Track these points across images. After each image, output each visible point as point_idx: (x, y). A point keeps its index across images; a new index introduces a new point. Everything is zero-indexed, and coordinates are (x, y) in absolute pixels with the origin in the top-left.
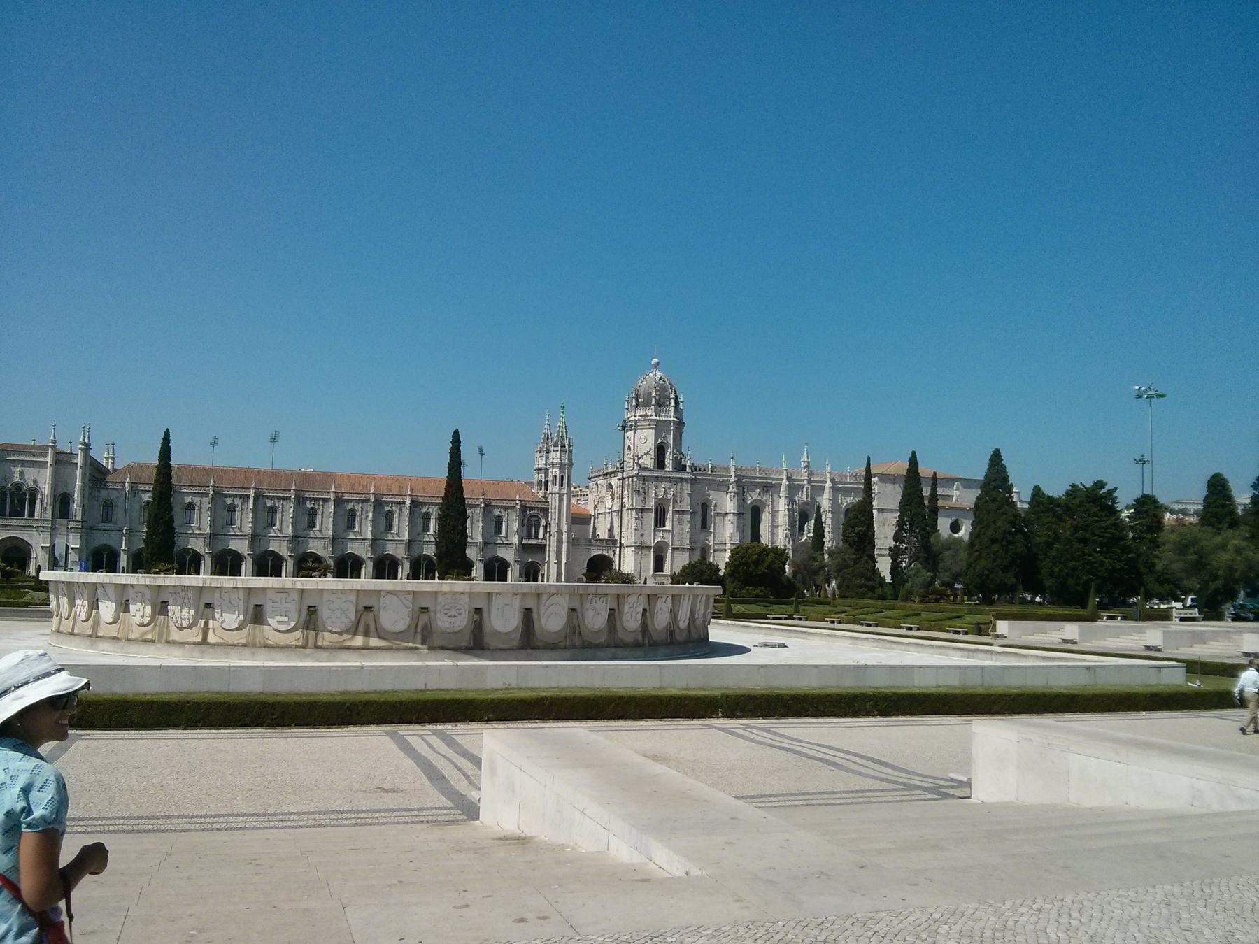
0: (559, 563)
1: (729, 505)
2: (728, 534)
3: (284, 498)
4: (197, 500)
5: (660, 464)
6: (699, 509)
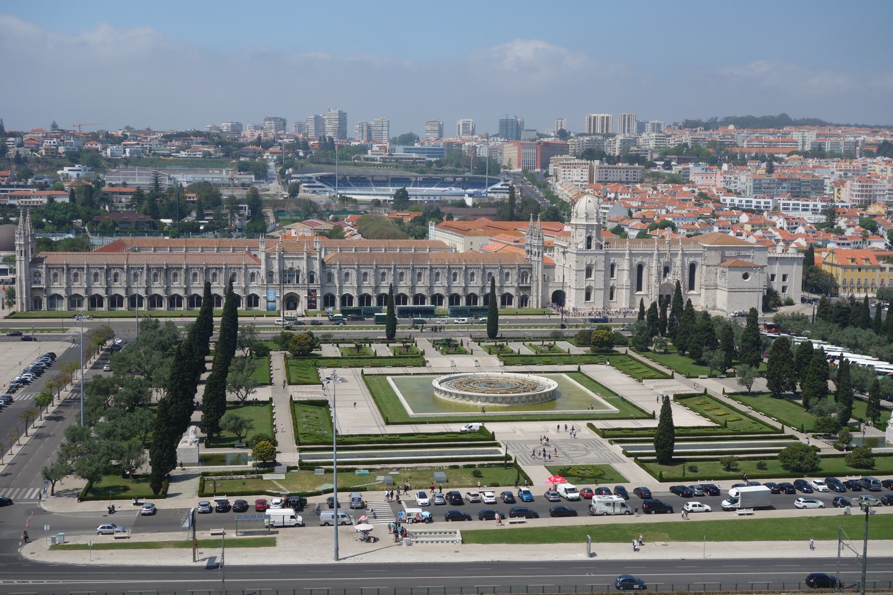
0: (537, 296)
1: (625, 265)
2: (624, 282)
3: (406, 268)
4: (368, 271)
5: (589, 246)
6: (610, 268)
